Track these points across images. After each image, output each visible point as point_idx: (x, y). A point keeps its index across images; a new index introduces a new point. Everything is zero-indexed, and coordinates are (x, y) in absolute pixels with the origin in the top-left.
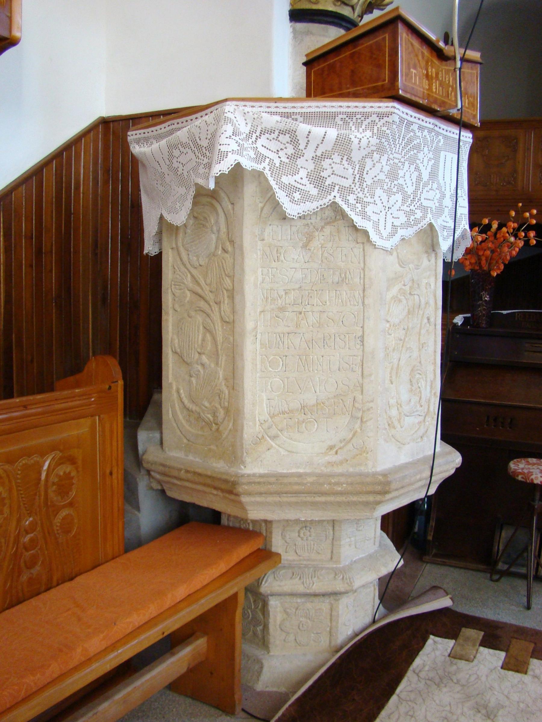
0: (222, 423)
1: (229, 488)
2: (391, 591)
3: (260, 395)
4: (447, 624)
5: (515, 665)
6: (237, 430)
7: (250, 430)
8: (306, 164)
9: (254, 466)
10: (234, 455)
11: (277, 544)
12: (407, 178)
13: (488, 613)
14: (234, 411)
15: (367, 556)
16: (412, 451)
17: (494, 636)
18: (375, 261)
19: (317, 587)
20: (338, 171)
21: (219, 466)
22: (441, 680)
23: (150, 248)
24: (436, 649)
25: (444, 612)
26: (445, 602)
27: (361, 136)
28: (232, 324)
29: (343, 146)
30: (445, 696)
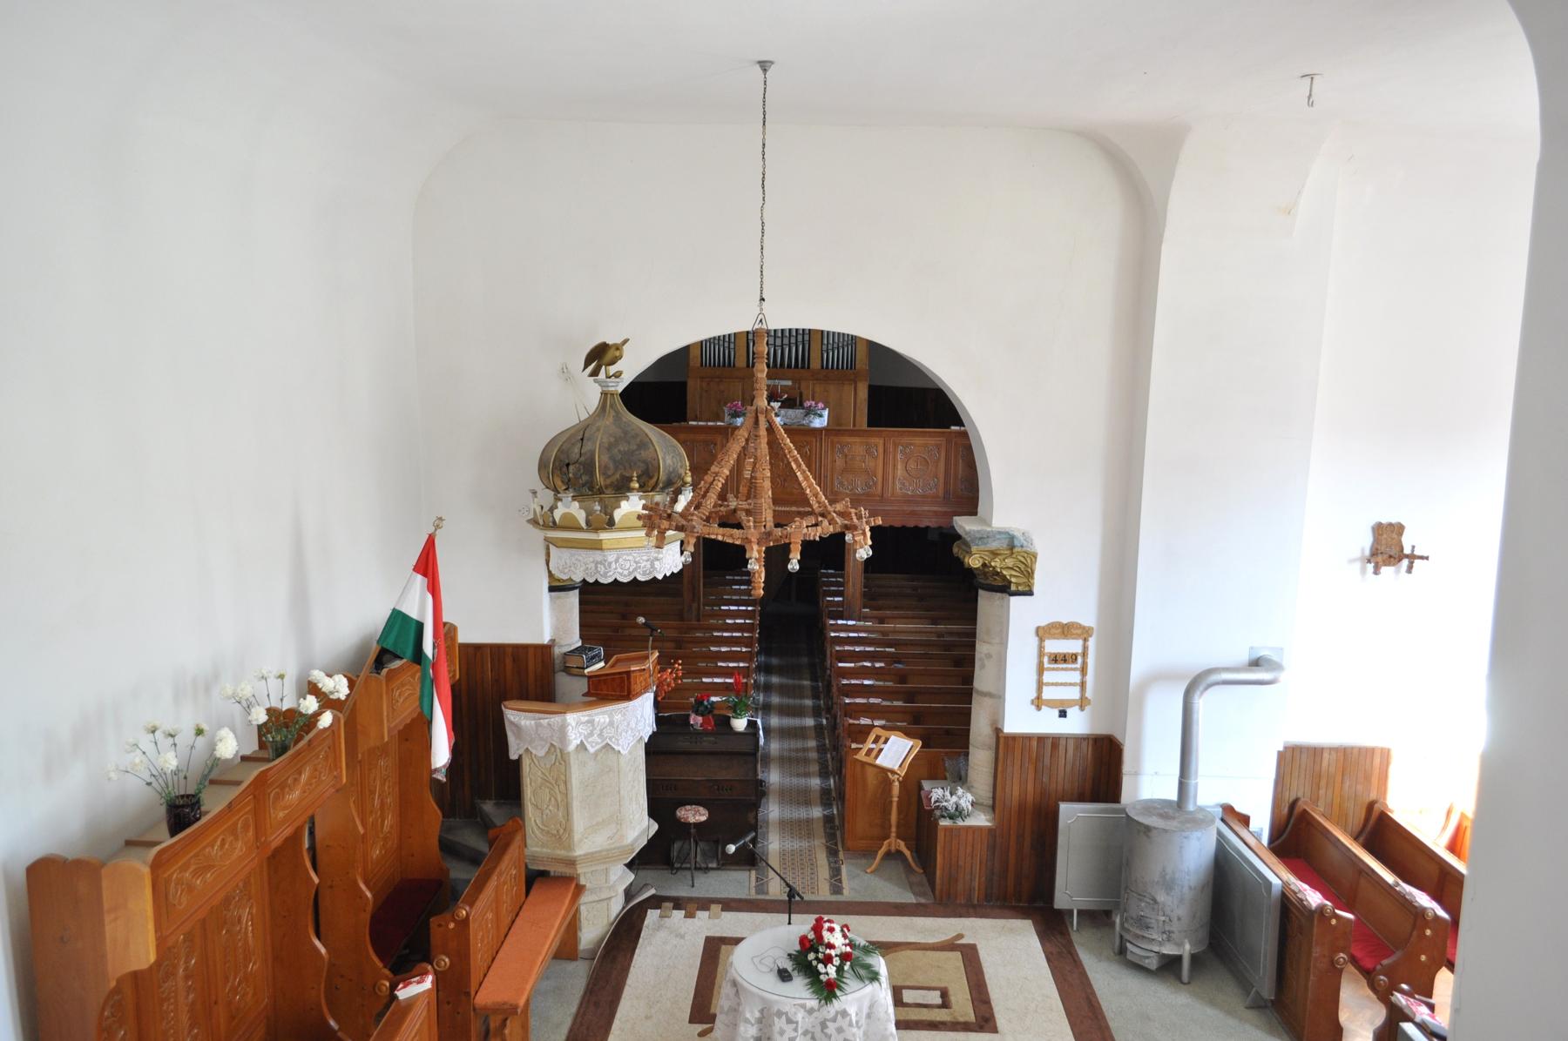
0: (563, 835)
1: (572, 863)
2: (629, 894)
3: (579, 823)
4: (656, 902)
5: (690, 915)
6: (570, 836)
7: (577, 837)
8: (597, 732)
9: (579, 852)
10: (570, 848)
11: (582, 882)
12: (633, 724)
13: (673, 893)
14: (568, 829)
15: (621, 878)
16: (639, 827)
17: (678, 903)
18: (622, 761)
19: (603, 896)
20: (608, 733)
21: (561, 853)
22: (659, 928)
23: (513, 756)
24: (652, 915)
25: (653, 896)
26: (652, 892)
27: (618, 717)
28: (566, 794)
29: (611, 724)
30: (662, 934)
